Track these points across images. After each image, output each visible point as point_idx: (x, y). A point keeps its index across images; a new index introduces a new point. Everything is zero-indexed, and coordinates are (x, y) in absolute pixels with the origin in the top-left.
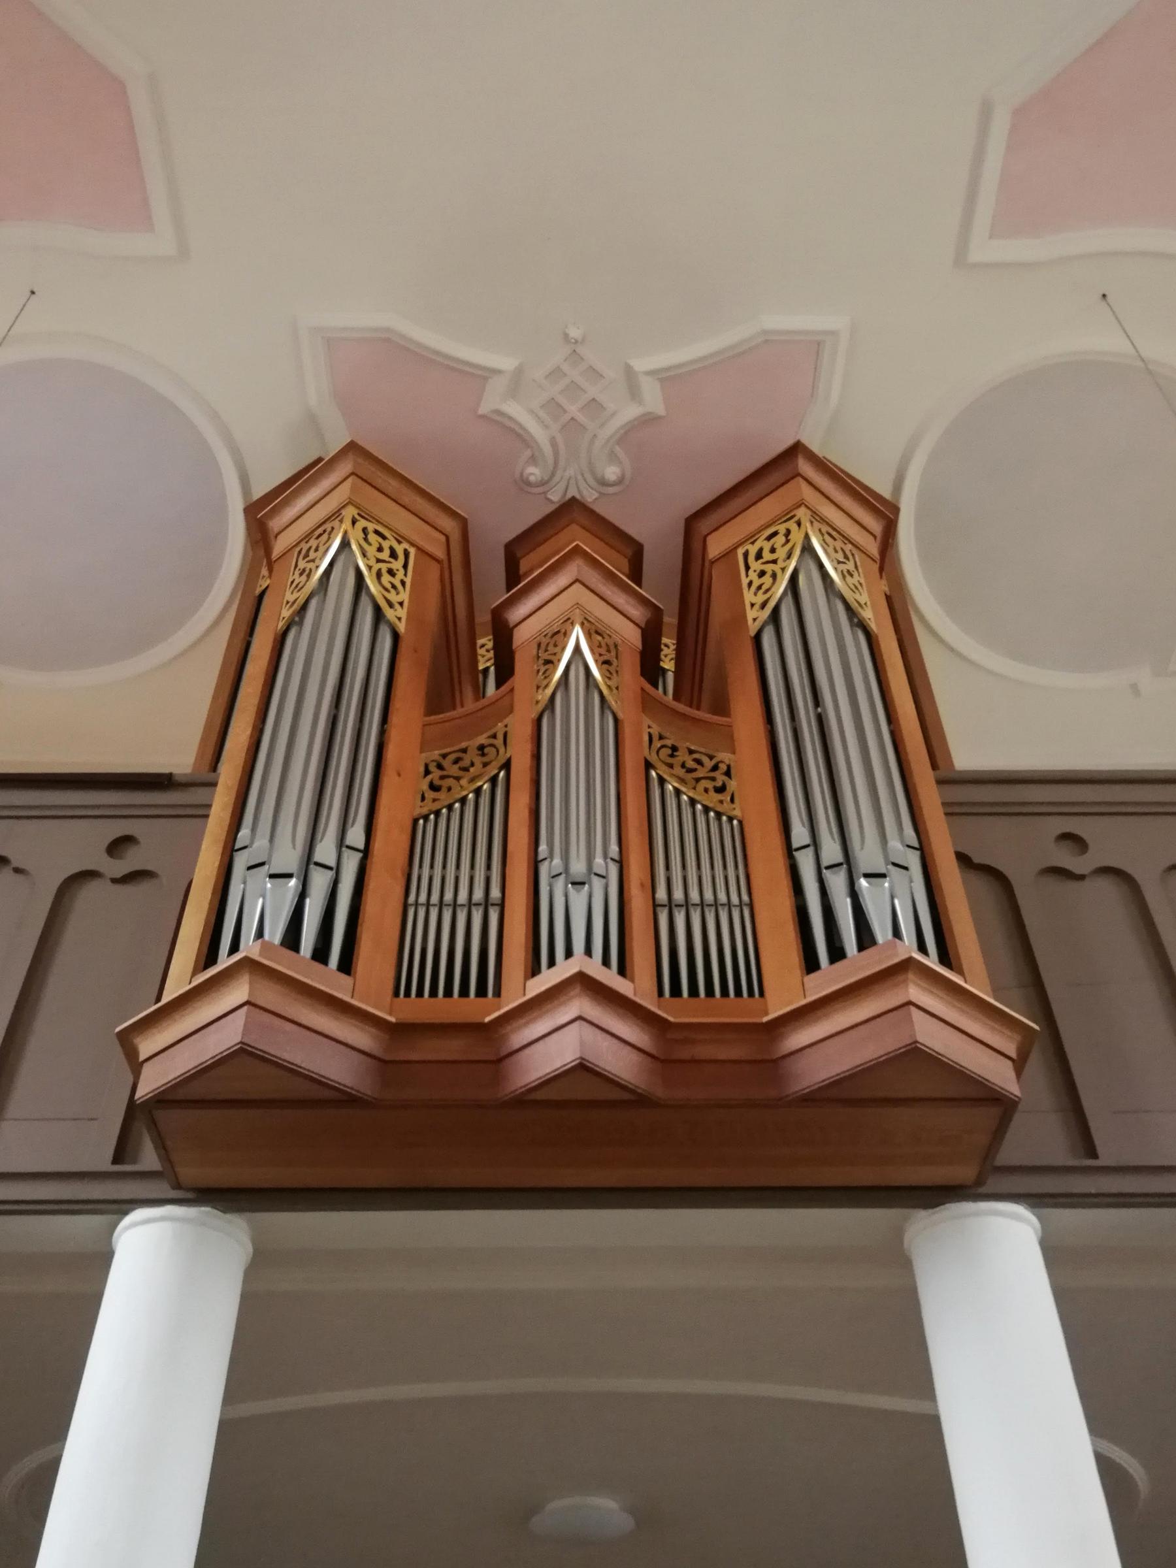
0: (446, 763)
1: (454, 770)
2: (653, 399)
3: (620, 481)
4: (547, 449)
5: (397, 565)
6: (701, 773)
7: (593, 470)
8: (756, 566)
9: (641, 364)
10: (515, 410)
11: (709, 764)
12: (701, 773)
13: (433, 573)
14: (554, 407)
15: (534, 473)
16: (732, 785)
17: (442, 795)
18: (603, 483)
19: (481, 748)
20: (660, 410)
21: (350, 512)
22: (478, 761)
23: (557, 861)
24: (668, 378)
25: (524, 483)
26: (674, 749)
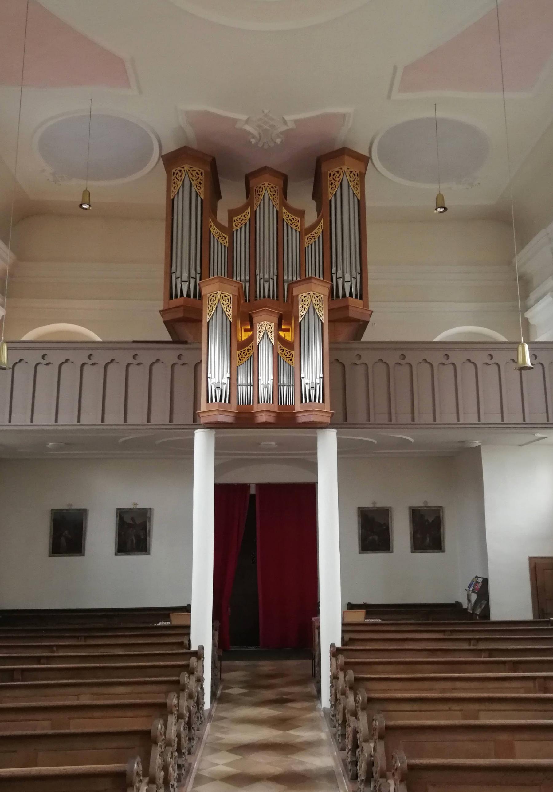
0: (242, 353)
1: (243, 356)
2: (291, 125)
3: (281, 142)
4: (257, 135)
5: (229, 303)
6: (288, 356)
7: (273, 162)
8: (302, 303)
9: (287, 118)
10: (248, 128)
11: (289, 354)
12: (288, 356)
13: (236, 297)
14: (259, 126)
15: (253, 141)
16: (293, 359)
17: (241, 361)
18: (275, 142)
19: (248, 350)
20: (295, 127)
21: (219, 293)
22: (248, 353)
23: (262, 274)
24: (296, 121)
25: (250, 142)
26: (283, 350)
